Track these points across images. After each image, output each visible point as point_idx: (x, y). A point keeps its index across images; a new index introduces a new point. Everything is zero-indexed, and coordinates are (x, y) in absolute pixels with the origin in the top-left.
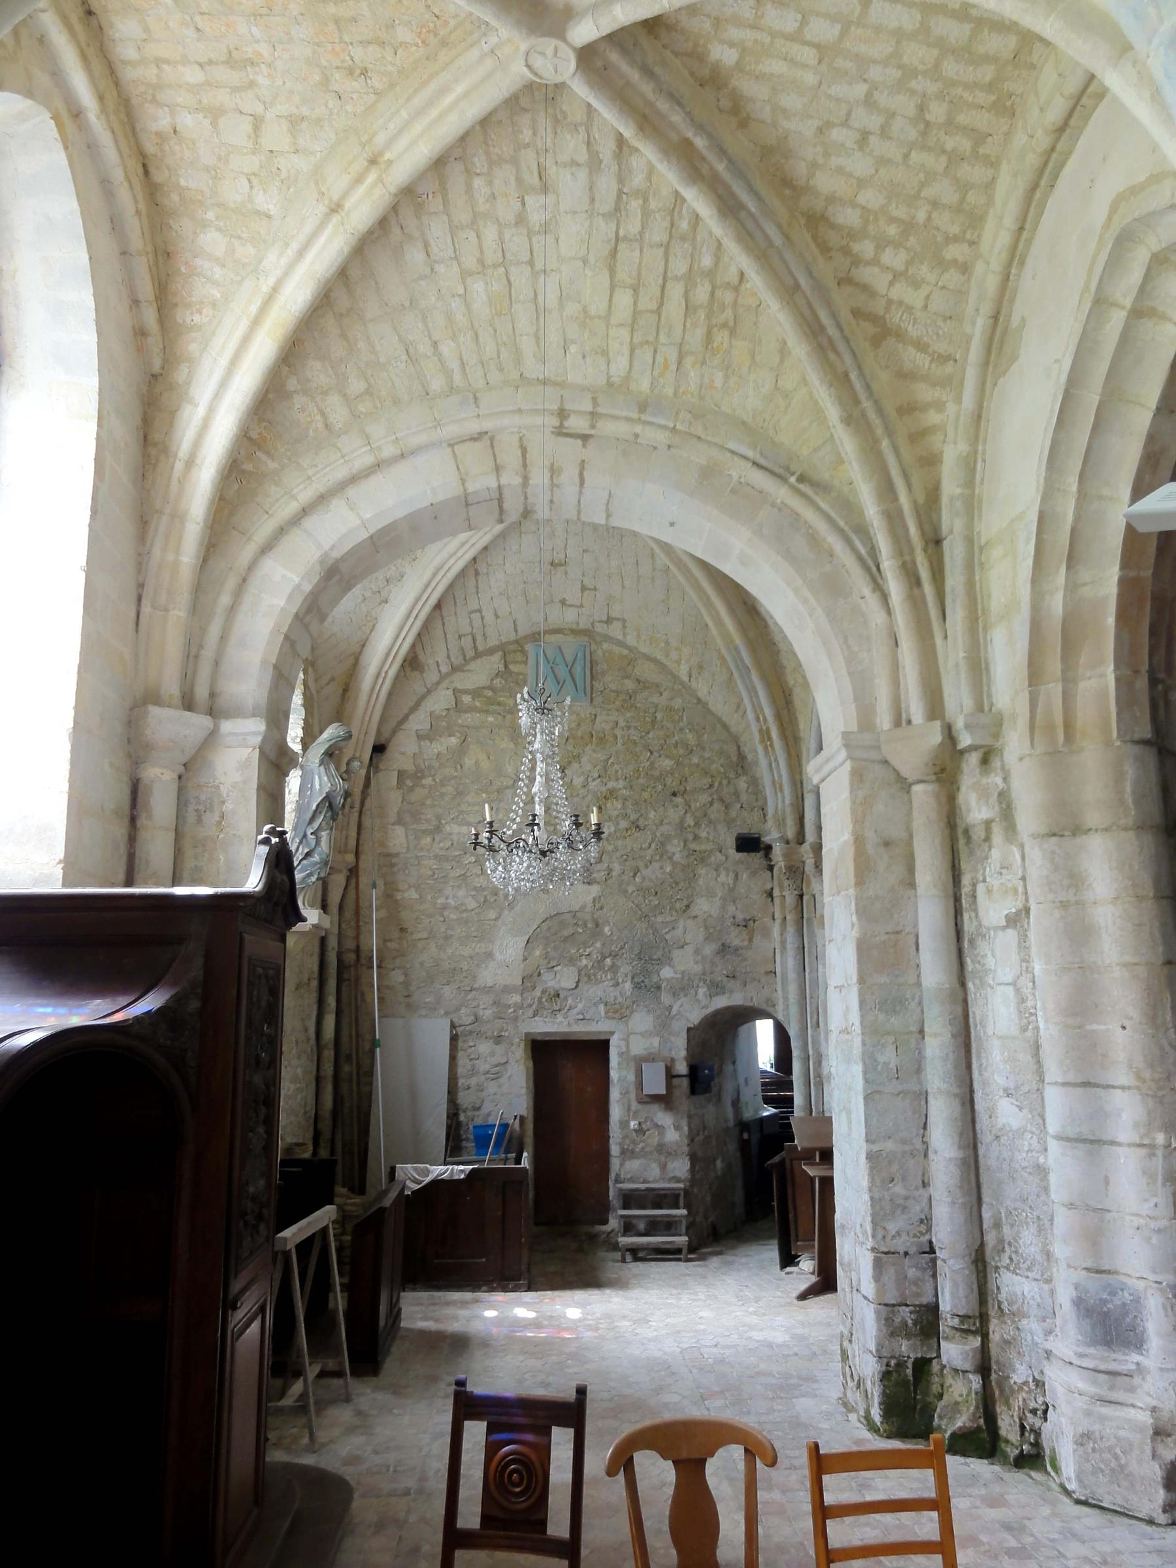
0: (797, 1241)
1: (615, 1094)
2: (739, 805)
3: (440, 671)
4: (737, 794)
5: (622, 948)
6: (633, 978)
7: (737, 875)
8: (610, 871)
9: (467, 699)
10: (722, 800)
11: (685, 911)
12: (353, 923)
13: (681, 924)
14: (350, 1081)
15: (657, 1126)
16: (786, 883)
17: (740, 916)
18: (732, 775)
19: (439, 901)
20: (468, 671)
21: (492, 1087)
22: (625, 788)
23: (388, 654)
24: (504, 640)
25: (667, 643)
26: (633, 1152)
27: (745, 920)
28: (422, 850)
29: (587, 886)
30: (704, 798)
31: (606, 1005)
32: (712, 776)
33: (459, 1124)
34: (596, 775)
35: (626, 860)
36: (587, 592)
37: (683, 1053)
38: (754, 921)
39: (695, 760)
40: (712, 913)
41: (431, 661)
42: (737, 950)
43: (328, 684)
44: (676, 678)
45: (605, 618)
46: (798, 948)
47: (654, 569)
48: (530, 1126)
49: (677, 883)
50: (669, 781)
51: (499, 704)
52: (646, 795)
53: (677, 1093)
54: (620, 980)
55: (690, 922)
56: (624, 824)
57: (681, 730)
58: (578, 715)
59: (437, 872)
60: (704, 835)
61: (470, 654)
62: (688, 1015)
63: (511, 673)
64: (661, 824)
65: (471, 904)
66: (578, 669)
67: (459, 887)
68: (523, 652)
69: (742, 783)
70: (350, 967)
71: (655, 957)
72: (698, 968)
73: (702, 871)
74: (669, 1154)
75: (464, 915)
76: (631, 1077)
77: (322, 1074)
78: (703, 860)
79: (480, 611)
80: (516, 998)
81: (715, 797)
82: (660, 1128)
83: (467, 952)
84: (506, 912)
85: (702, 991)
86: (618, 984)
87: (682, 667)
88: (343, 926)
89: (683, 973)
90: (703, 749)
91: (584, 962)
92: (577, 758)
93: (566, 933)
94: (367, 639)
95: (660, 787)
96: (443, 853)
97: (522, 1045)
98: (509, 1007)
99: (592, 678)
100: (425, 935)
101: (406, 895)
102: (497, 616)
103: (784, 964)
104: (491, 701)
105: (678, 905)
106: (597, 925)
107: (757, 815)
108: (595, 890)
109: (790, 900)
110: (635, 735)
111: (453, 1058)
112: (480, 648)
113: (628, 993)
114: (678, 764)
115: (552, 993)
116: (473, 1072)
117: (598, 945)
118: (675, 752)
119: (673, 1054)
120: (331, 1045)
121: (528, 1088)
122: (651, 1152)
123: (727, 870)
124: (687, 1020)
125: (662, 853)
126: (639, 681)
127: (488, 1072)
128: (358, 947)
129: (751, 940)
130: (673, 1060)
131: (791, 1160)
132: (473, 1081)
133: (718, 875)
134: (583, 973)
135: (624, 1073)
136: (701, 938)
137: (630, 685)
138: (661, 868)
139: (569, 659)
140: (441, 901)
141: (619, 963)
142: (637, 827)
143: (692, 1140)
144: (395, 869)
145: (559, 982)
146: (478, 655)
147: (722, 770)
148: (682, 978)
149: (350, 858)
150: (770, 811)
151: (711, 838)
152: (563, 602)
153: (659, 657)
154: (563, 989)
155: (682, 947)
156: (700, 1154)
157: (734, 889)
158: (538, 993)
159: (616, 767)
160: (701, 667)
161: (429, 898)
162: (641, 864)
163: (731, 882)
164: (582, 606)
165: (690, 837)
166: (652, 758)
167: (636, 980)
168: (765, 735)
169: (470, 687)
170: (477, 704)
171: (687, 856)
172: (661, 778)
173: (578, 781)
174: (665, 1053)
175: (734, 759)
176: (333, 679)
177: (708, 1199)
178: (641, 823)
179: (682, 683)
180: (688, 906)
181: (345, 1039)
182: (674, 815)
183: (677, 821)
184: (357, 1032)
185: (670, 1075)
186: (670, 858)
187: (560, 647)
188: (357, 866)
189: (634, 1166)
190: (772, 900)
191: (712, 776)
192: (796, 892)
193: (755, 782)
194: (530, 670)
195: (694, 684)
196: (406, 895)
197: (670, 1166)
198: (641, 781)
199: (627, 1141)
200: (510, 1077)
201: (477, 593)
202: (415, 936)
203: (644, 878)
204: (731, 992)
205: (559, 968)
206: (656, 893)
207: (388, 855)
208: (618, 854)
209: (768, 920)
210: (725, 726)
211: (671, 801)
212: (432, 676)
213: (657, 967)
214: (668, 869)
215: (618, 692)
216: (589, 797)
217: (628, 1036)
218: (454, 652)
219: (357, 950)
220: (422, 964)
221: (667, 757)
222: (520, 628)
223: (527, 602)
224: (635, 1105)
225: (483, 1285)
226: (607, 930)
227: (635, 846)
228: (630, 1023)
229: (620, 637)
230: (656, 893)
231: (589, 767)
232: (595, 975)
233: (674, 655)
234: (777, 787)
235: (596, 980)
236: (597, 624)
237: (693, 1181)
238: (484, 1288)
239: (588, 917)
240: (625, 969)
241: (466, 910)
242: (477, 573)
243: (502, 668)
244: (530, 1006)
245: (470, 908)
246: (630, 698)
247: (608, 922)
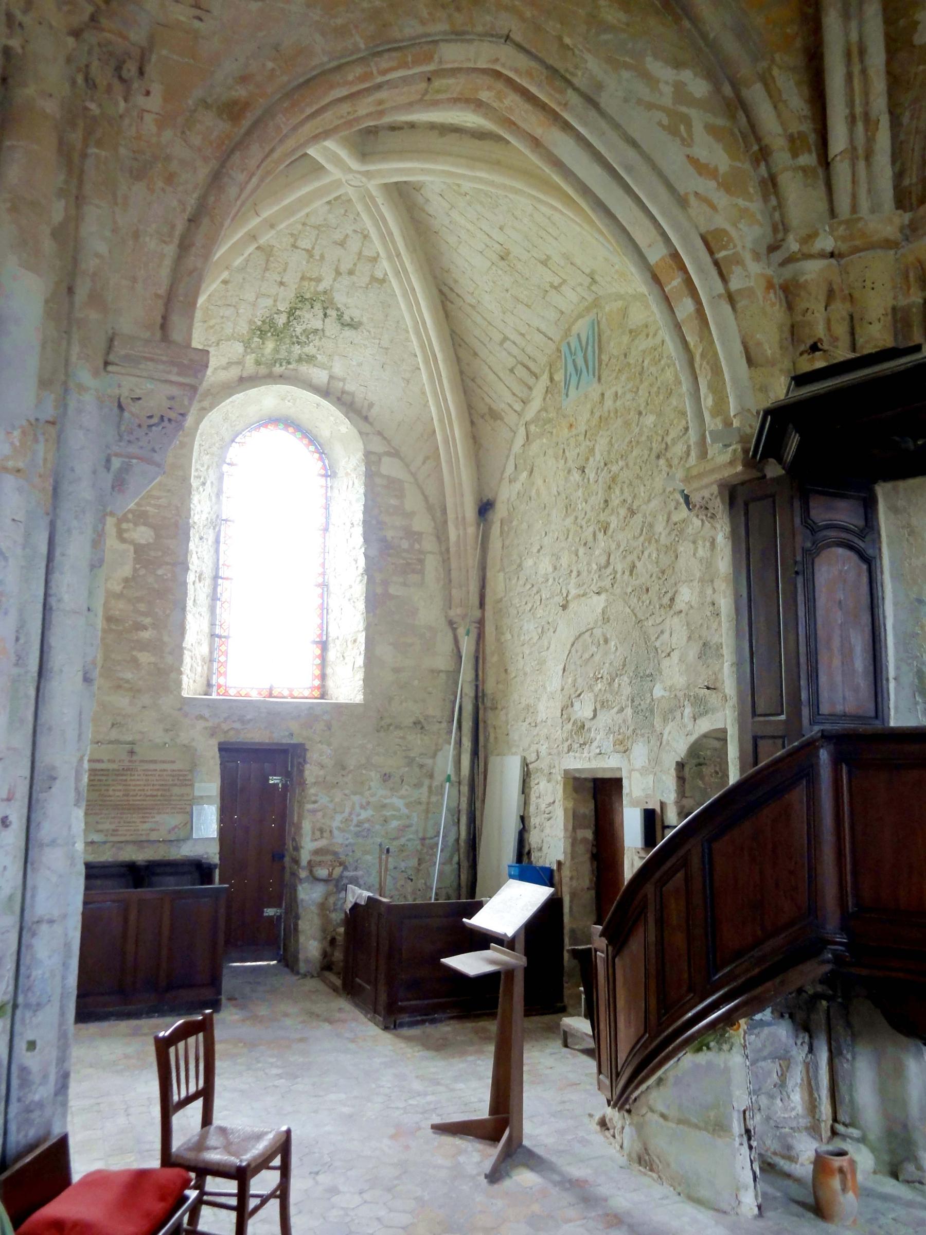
3: (516, 411)
41: (503, 406)
79: (506, 339)
102: (523, 335)
155: (669, 655)
180: (672, 600)
212: (511, 419)
218: (516, 388)
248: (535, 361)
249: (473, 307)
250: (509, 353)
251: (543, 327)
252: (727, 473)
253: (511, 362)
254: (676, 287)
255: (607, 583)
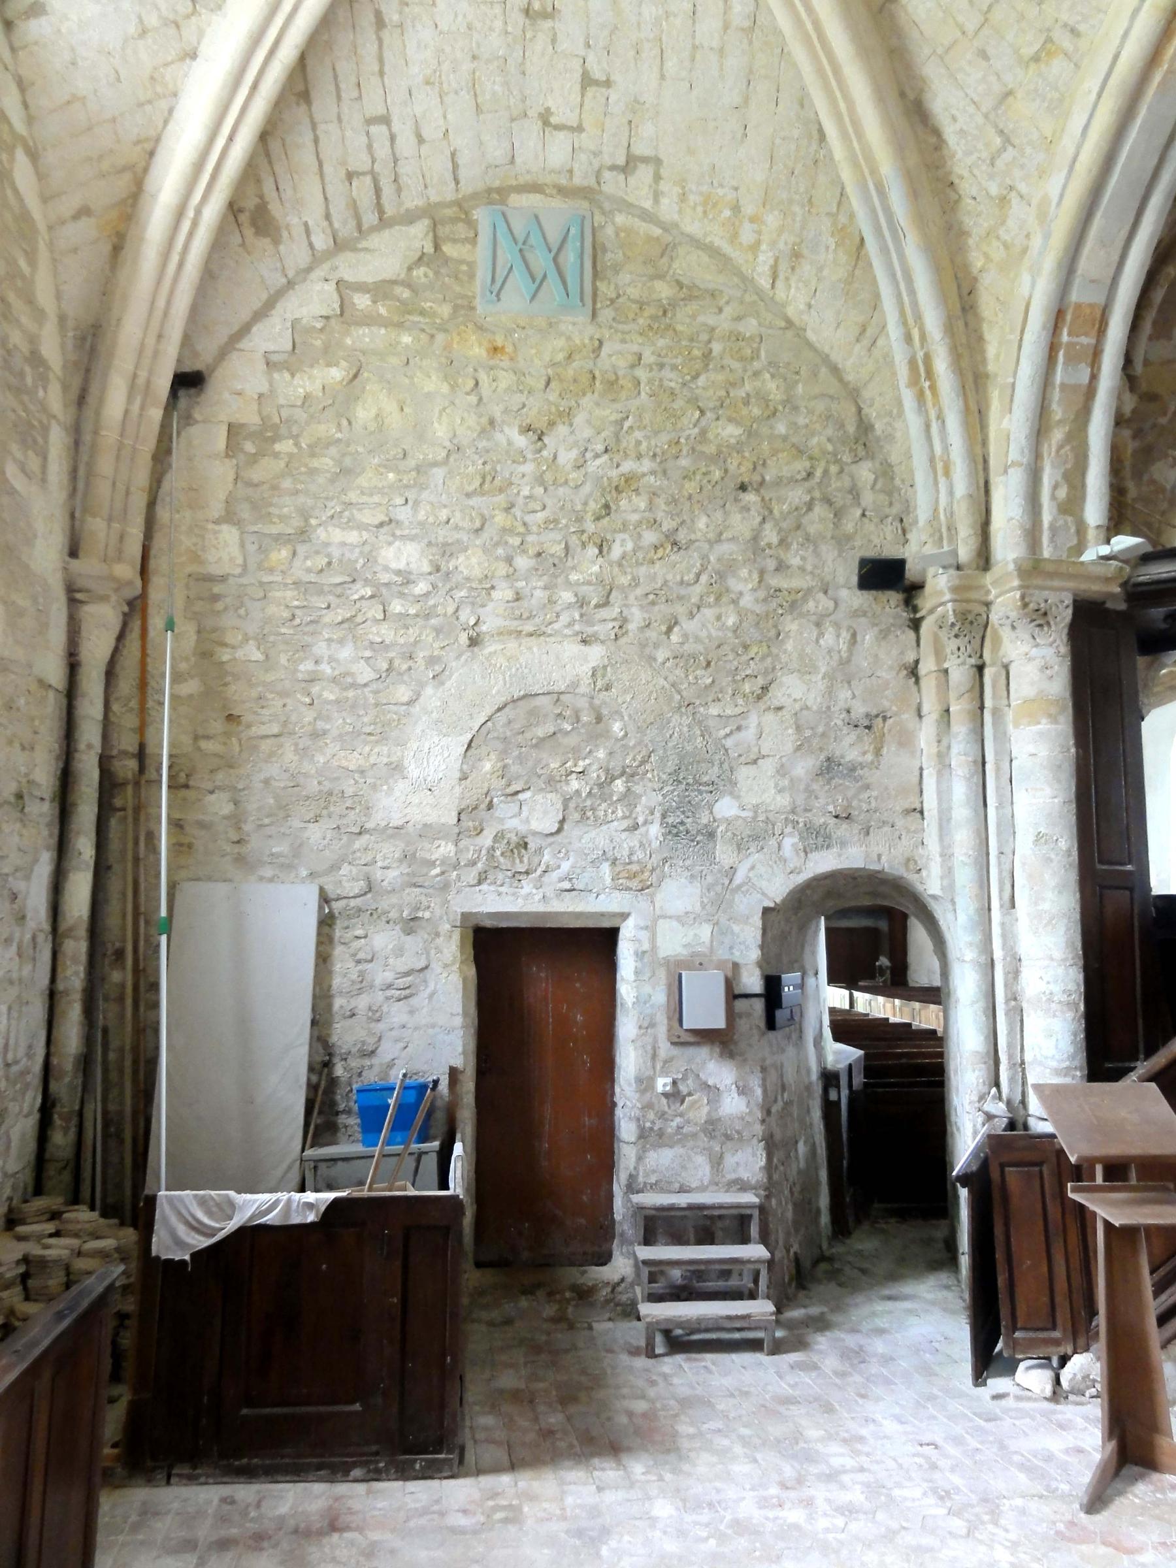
0: (1015, 1329)
1: (627, 1028)
2: (859, 512)
3: (311, 245)
4: (854, 493)
5: (643, 763)
6: (664, 816)
7: (854, 635)
8: (623, 621)
9: (362, 301)
10: (828, 501)
11: (759, 698)
12: (134, 704)
13: (753, 720)
14: (121, 999)
15: (706, 1087)
16: (952, 645)
17: (860, 710)
18: (847, 458)
19: (302, 667)
20: (366, 249)
21: (397, 1014)
22: (653, 473)
23: (198, 166)
24: (434, 198)
25: (736, 208)
26: (661, 1134)
27: (867, 715)
28: (271, 570)
29: (582, 647)
30: (797, 495)
31: (614, 862)
32: (811, 458)
33: (333, 1082)
34: (600, 448)
35: (653, 603)
36: (591, 91)
37: (755, 954)
38: (885, 719)
39: (781, 428)
40: (809, 704)
41: (294, 221)
42: (853, 769)
43: (76, 217)
44: (747, 282)
45: (621, 161)
46: (975, 762)
47: (726, 27)
48: (468, 1086)
49: (746, 647)
50: (733, 464)
51: (422, 313)
52: (690, 487)
53: (743, 1025)
54: (640, 820)
55: (770, 717)
56: (650, 537)
57: (756, 374)
58: (569, 338)
59: (298, 612)
60: (795, 561)
61: (370, 218)
62: (764, 884)
63: (446, 260)
64: (719, 540)
65: (365, 674)
66: (570, 257)
67: (341, 642)
68: (471, 223)
69: (865, 473)
70: (124, 784)
71: (705, 779)
72: (783, 801)
73: (791, 626)
74: (728, 1137)
75: (351, 694)
76: (660, 997)
77: (60, 986)
78: (793, 605)
79: (385, 120)
80: (446, 849)
81: (817, 494)
82: (713, 1092)
83: (354, 761)
84: (429, 691)
85: (790, 842)
86: (636, 827)
87: (761, 258)
88: (115, 707)
89: (756, 809)
90: (796, 408)
91: (575, 784)
92: (567, 415)
93: (540, 732)
94: (158, 140)
95: (717, 474)
96: (312, 578)
97: (456, 936)
98: (433, 864)
99: (596, 275)
100: (275, 729)
101: (240, 654)
102: (421, 140)
103: (943, 795)
104: (406, 308)
105: (747, 687)
106: (599, 719)
107: (890, 529)
108: (596, 654)
109: (960, 674)
110: (672, 379)
111: (323, 959)
112: (390, 211)
113: (655, 844)
114: (750, 433)
115: (514, 839)
116: (362, 985)
117: (601, 754)
118: (745, 412)
119: (737, 956)
120: (82, 932)
121: (465, 1014)
122: (694, 1136)
123: (837, 625)
124: (764, 894)
125: (720, 593)
126: (680, 285)
127: (389, 986)
128: (142, 747)
129: (878, 752)
130: (736, 966)
131: (1002, 1166)
132: (362, 1003)
133: (821, 635)
134: (572, 805)
135: (647, 989)
136: (789, 747)
137: (664, 291)
138: (719, 618)
139: (554, 237)
140: (306, 666)
141: (638, 789)
142: (675, 543)
143: (769, 1112)
144: (219, 606)
145: (527, 821)
146: (384, 222)
147: (830, 448)
148: (755, 818)
149: (127, 571)
150: (922, 513)
151: (809, 568)
152: (545, 118)
153: (718, 242)
154: (535, 833)
155: (755, 762)
156: (778, 1136)
157: (849, 661)
158: (486, 840)
159: (638, 435)
160: (796, 255)
161: (283, 660)
162: (680, 610)
163: (843, 647)
164: (579, 129)
165: (771, 564)
166: (703, 422)
167: (670, 820)
168: (920, 372)
169: (370, 280)
170: (383, 311)
171: (765, 600)
172: (719, 457)
173: (567, 457)
174: (722, 954)
175: (851, 429)
176: (84, 212)
177: (789, 1215)
178: (682, 536)
179: (759, 292)
180: (765, 689)
181: (112, 920)
182: (741, 524)
183: (748, 535)
184: (136, 907)
185: (733, 995)
186: (735, 602)
187: (536, 217)
188: (144, 596)
189: (662, 1159)
190: (917, 682)
191: (811, 458)
192: (973, 661)
193: (886, 472)
194: (481, 253)
195: (780, 294)
196: (240, 654)
197: (730, 1160)
198: (684, 462)
199: (651, 1115)
200: (431, 996)
201: (381, 73)
202: (255, 731)
203: (685, 636)
204: (843, 844)
205: (527, 795)
206: (708, 664)
207: (209, 579)
208: (639, 591)
209: (908, 717)
210: (835, 370)
211: (736, 500)
212: (295, 254)
213: (707, 797)
214: (731, 621)
215: (642, 305)
216: (587, 488)
217: (655, 920)
218: (339, 210)
219: (141, 755)
220: (267, 782)
221: (730, 420)
222: (463, 173)
223: (478, 109)
224: (665, 1049)
225: (354, 1465)
226: (617, 727)
227: (669, 577)
228: (659, 897)
229: (648, 204)
230: (708, 664)
231: (587, 433)
232: (593, 809)
233: (747, 235)
234: (939, 467)
235: (596, 818)
236: (607, 175)
237: (770, 1188)
238: (357, 1473)
239: (583, 703)
240: (649, 799)
241: (354, 685)
242: (380, 22)
243: (429, 248)
244: (473, 863)
245: (362, 680)
246: (665, 312)
247: (617, 712)
248: (399, 190)
249: (380, 23)
250: (370, 147)
251: (463, 160)
252: (1095, 589)
253: (360, 161)
254: (1082, 345)
255: (604, 629)
